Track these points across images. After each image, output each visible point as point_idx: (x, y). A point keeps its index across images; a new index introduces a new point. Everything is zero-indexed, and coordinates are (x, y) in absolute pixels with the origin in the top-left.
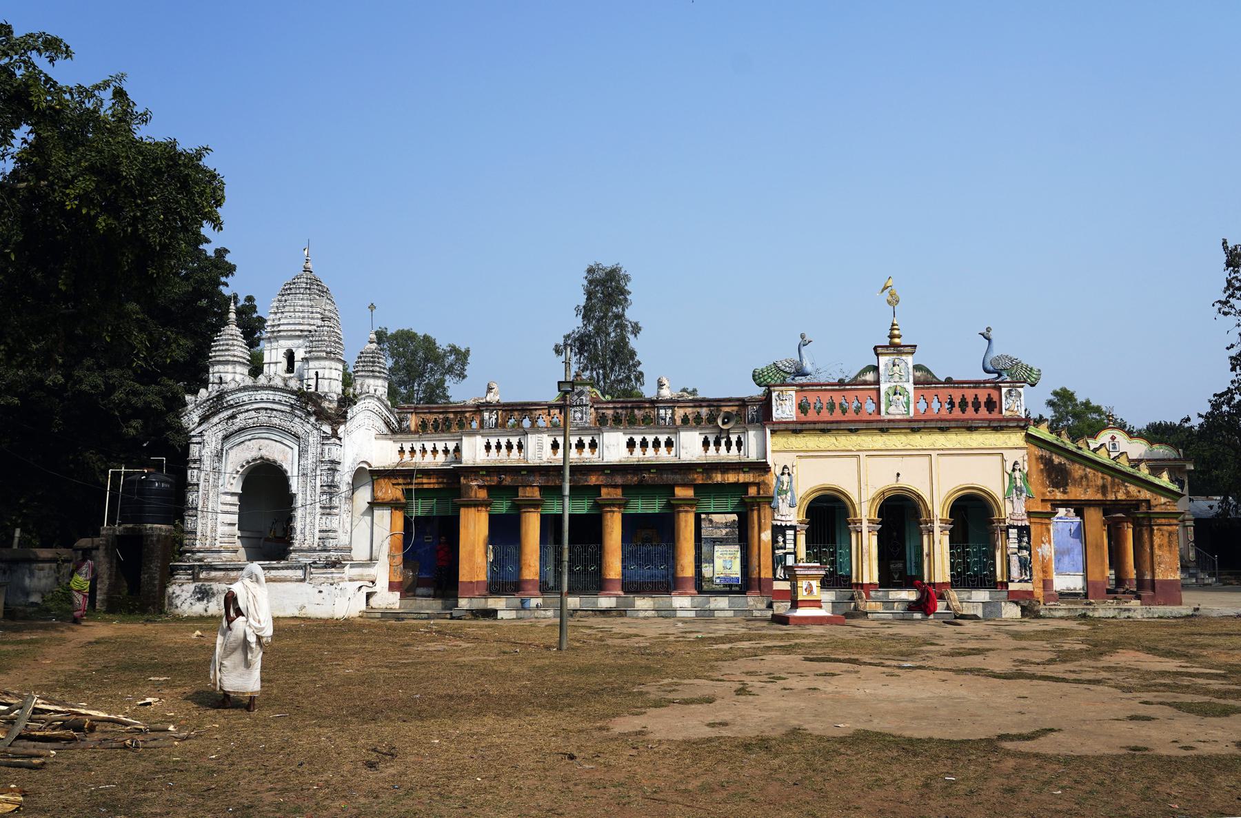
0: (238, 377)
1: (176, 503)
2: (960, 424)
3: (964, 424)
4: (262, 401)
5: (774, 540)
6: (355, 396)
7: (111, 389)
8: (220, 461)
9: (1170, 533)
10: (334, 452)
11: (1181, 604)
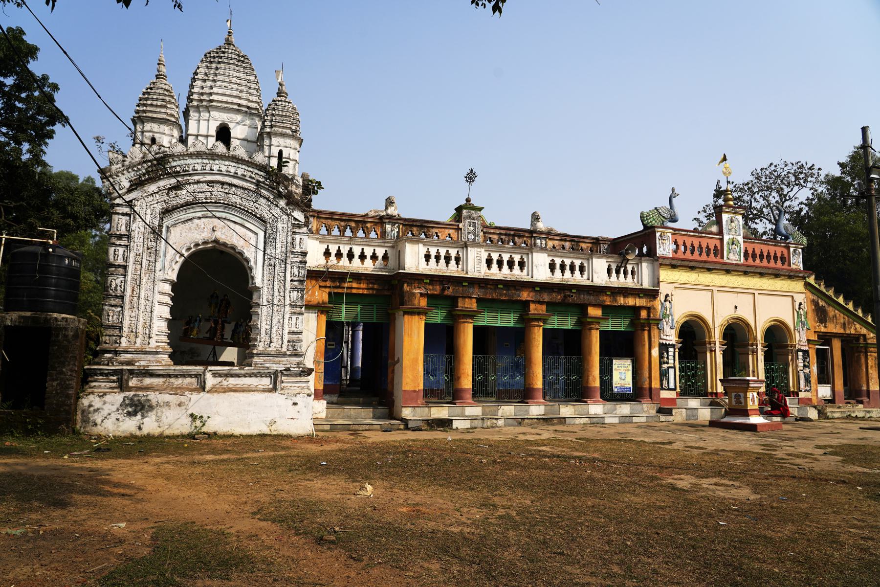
4: (219, 173)
5: (661, 356)
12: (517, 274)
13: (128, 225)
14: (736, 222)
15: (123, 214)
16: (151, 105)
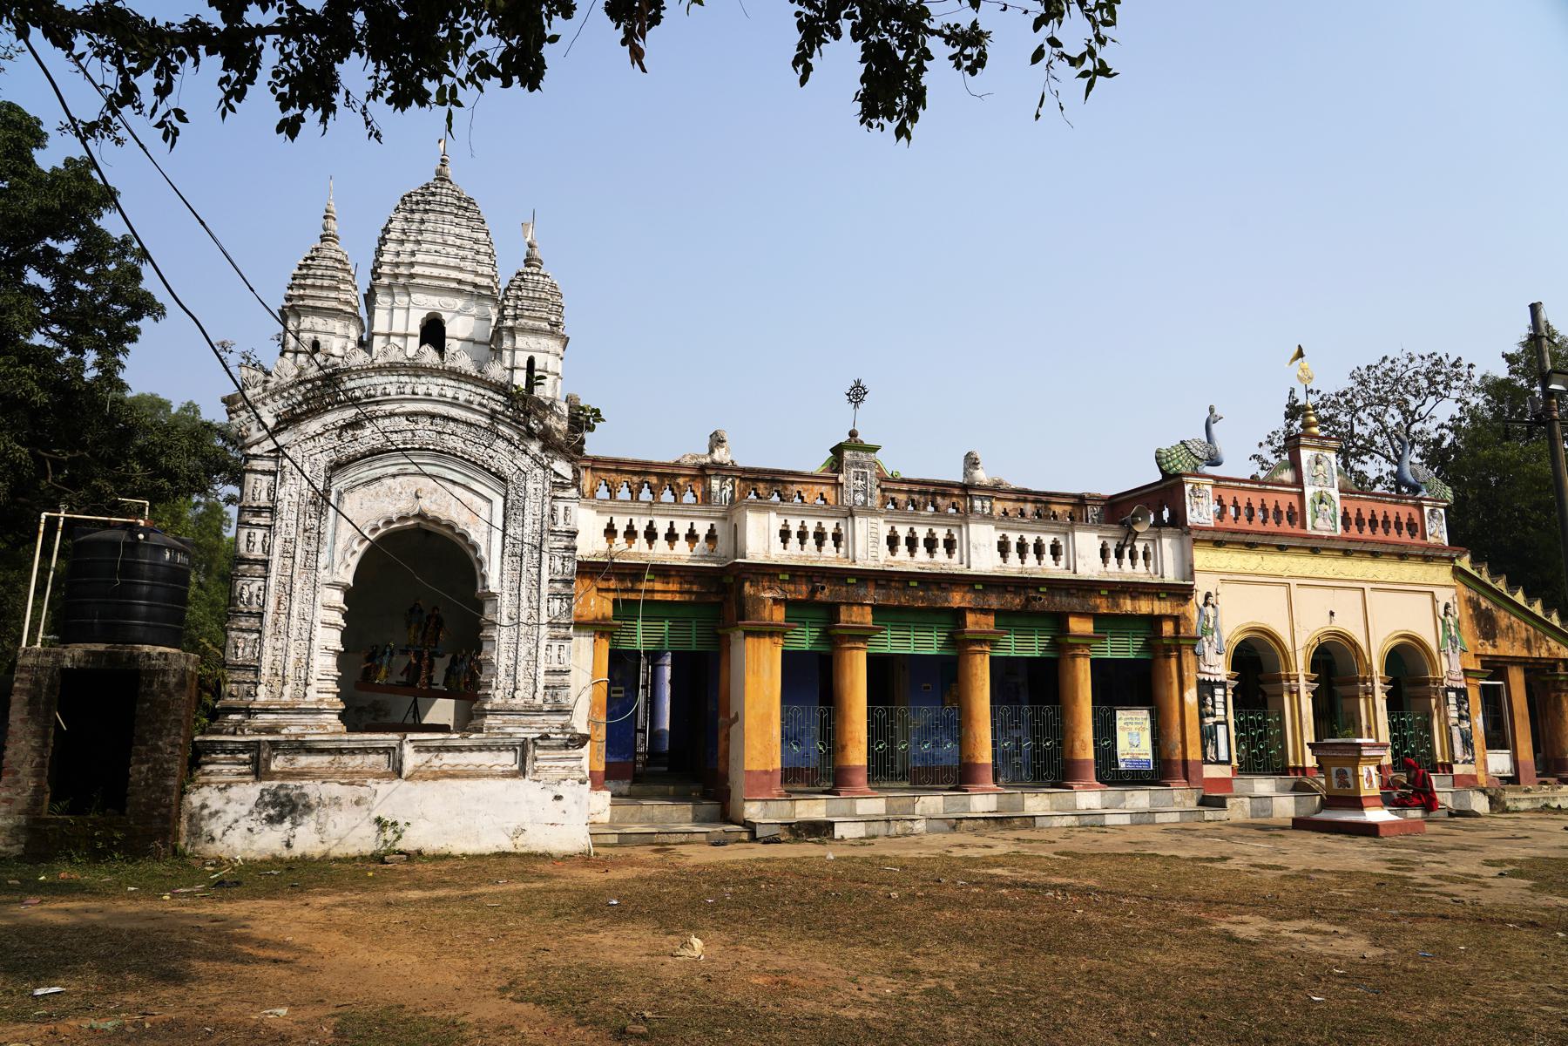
4: (428, 397)
5: (1202, 703)
12: (942, 561)
13: (272, 491)
14: (1325, 463)
15: (263, 472)
16: (313, 286)
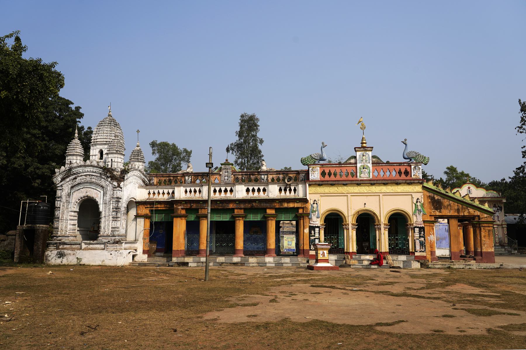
0: (78, 162)
1: (50, 215)
2: (392, 182)
3: (395, 182)
4: (88, 172)
5: (310, 233)
6: (128, 170)
7: (27, 166)
8: (69, 197)
9: (489, 231)
10: (118, 194)
11: (494, 263)
12: (229, 195)
14: (367, 156)
